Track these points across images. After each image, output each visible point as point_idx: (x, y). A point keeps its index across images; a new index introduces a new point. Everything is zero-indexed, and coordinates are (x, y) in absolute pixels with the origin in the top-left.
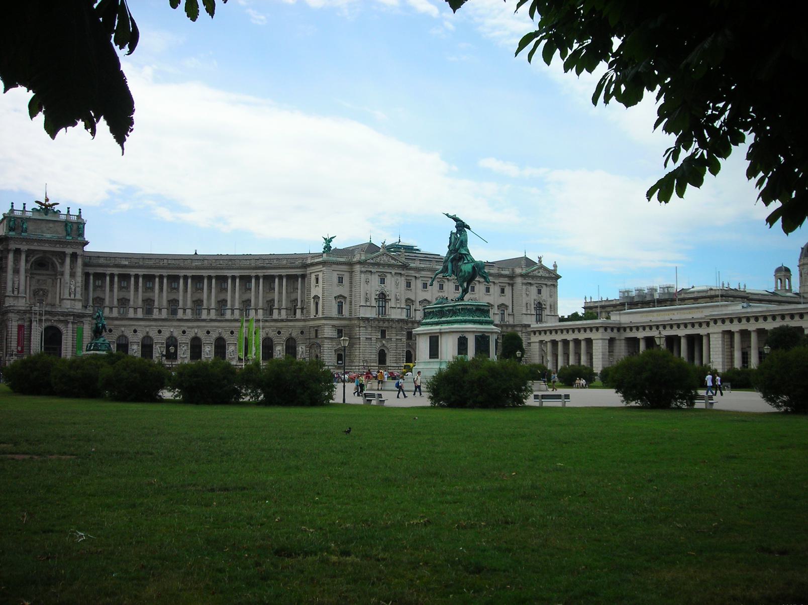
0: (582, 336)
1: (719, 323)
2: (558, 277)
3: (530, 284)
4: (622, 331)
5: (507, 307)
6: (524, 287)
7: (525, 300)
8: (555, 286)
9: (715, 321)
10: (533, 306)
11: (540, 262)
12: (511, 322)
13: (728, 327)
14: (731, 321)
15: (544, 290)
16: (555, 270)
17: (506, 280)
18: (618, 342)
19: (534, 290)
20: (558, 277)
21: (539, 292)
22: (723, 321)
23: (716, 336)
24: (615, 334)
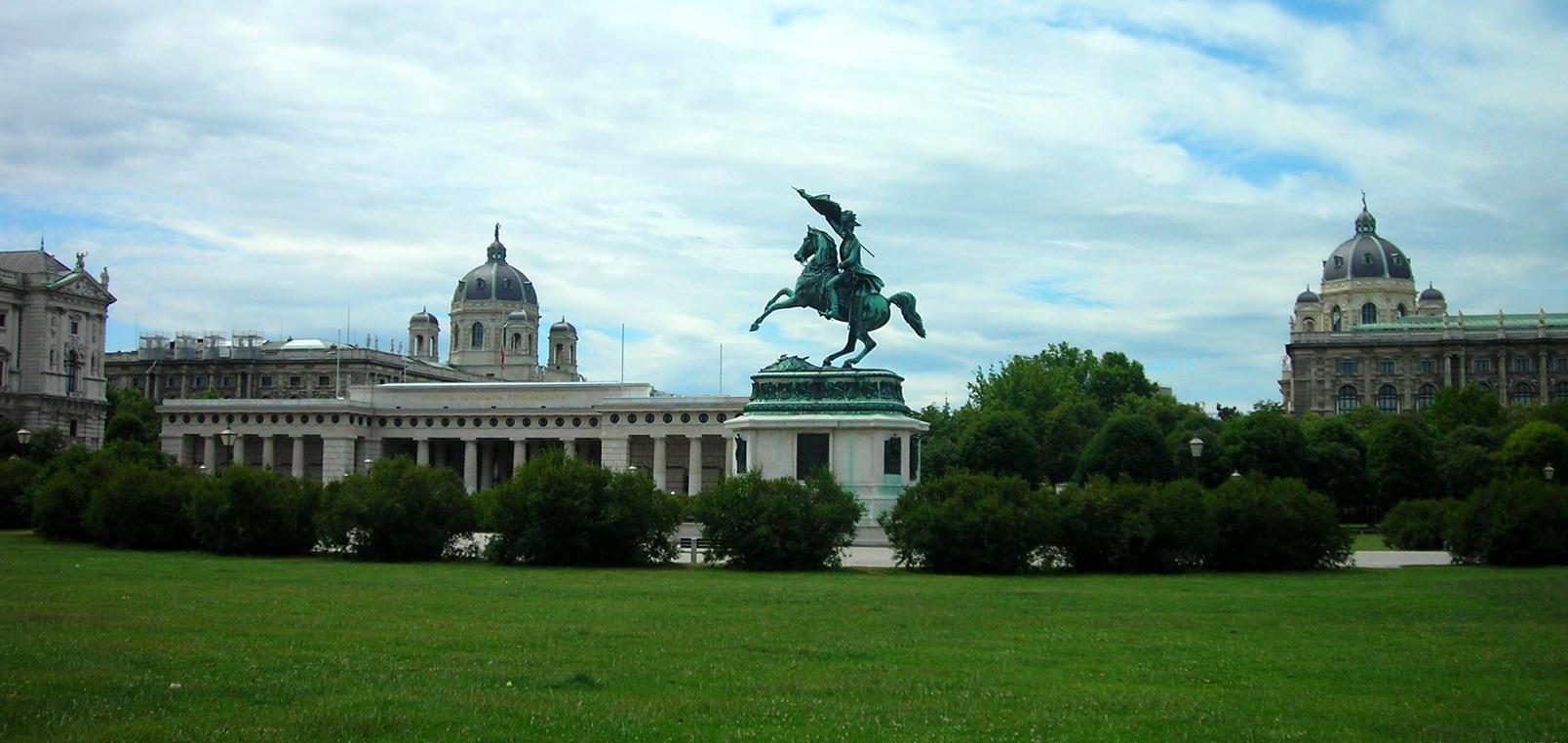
0: (296, 430)
1: (623, 420)
2: (111, 300)
3: (61, 311)
4: (376, 424)
5: (8, 354)
6: (50, 316)
7: (50, 342)
8: (102, 318)
9: (615, 418)
10: (62, 358)
11: (81, 265)
12: (15, 389)
13: (640, 428)
14: (650, 418)
15: (83, 324)
16: (105, 285)
17: (10, 298)
18: (368, 446)
19: (65, 323)
20: (111, 300)
21: (75, 328)
22: (632, 418)
23: (614, 444)
24: (363, 430)
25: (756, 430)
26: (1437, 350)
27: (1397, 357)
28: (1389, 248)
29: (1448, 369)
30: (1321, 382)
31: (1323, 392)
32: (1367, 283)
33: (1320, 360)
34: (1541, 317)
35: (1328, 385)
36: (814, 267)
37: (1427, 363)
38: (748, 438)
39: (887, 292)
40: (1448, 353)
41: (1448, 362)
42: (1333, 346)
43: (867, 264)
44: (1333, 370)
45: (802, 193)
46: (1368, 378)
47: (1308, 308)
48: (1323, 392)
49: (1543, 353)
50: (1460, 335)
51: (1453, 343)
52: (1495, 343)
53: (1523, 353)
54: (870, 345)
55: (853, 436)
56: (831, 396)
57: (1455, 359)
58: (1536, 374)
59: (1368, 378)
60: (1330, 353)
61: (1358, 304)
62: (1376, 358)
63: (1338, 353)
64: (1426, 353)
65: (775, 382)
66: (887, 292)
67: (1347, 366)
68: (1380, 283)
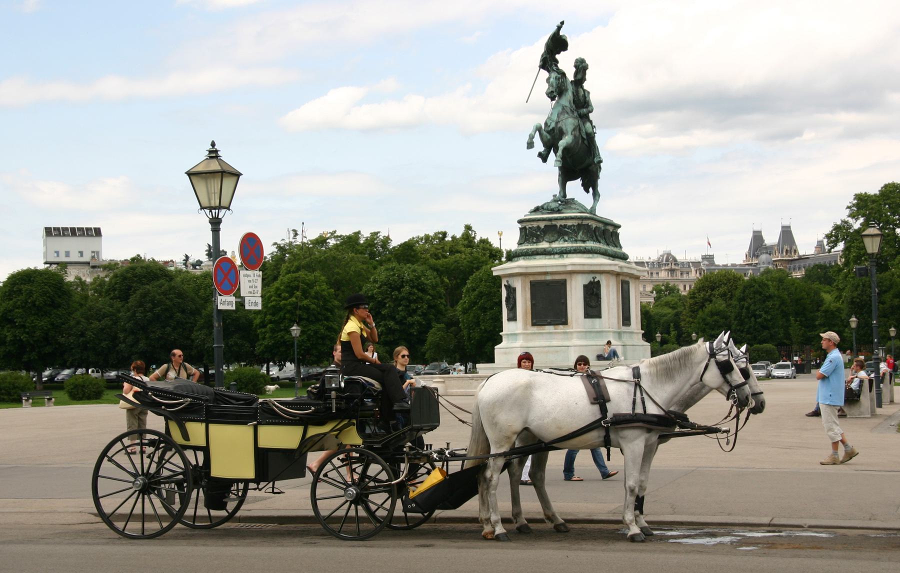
45: (559, 28)
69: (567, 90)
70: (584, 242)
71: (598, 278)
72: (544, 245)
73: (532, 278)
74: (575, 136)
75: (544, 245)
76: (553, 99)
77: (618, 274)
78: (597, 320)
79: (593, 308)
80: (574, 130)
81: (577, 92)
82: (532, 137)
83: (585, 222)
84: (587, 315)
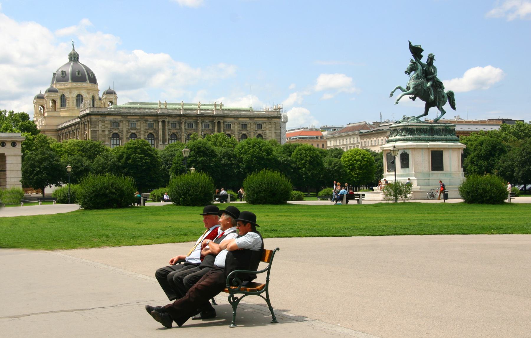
25: (414, 149)
26: (155, 118)
27: (138, 121)
28: (88, 70)
29: (160, 127)
30: (104, 131)
31: (105, 136)
32: (79, 84)
33: (103, 121)
34: (199, 105)
35: (107, 133)
36: (418, 77)
37: (150, 125)
38: (410, 153)
39: (446, 91)
40: (160, 120)
41: (160, 124)
42: (109, 114)
43: (439, 76)
44: (109, 126)
45: (410, 43)
46: (125, 130)
47: (54, 96)
48: (105, 136)
49: (200, 121)
50: (166, 112)
51: (162, 115)
52: (180, 116)
53: (191, 121)
54: (443, 112)
55: (451, 151)
56: (437, 134)
57: (163, 122)
58: (196, 130)
59: (125, 130)
60: (108, 118)
61: (75, 94)
62: (128, 121)
63: (111, 118)
64: (150, 119)
65: (415, 128)
66: (446, 91)
67: (116, 124)
68: (84, 85)
69: (418, 69)
70: (405, 136)
71: (407, 151)
72: (393, 138)
73: (387, 152)
74: (416, 90)
75: (393, 138)
76: (409, 74)
77: (429, 149)
78: (407, 169)
79: (405, 164)
80: (415, 86)
81: (429, 68)
82: (393, 92)
83: (406, 127)
84: (402, 167)
